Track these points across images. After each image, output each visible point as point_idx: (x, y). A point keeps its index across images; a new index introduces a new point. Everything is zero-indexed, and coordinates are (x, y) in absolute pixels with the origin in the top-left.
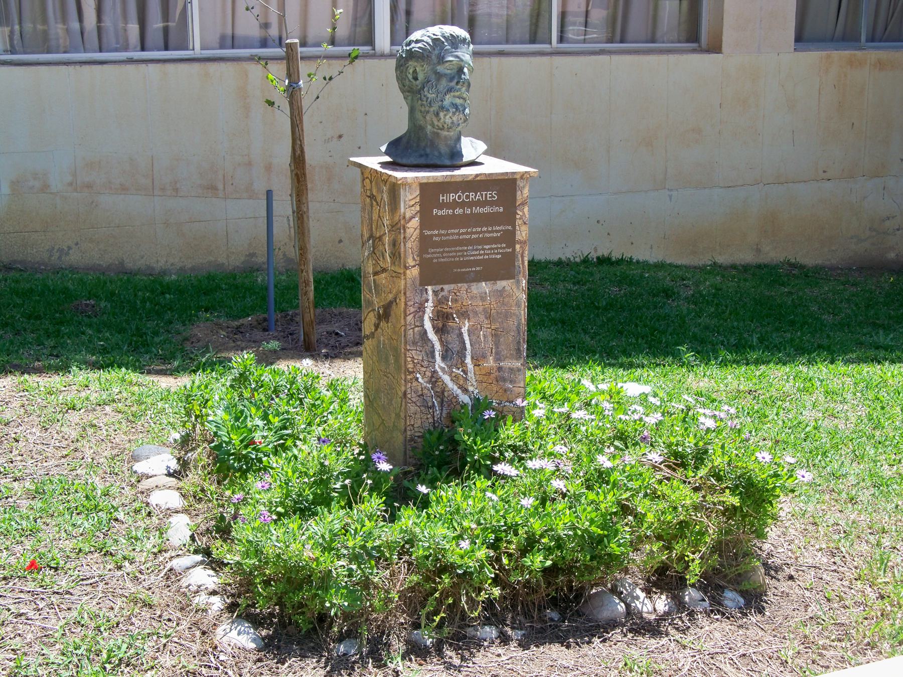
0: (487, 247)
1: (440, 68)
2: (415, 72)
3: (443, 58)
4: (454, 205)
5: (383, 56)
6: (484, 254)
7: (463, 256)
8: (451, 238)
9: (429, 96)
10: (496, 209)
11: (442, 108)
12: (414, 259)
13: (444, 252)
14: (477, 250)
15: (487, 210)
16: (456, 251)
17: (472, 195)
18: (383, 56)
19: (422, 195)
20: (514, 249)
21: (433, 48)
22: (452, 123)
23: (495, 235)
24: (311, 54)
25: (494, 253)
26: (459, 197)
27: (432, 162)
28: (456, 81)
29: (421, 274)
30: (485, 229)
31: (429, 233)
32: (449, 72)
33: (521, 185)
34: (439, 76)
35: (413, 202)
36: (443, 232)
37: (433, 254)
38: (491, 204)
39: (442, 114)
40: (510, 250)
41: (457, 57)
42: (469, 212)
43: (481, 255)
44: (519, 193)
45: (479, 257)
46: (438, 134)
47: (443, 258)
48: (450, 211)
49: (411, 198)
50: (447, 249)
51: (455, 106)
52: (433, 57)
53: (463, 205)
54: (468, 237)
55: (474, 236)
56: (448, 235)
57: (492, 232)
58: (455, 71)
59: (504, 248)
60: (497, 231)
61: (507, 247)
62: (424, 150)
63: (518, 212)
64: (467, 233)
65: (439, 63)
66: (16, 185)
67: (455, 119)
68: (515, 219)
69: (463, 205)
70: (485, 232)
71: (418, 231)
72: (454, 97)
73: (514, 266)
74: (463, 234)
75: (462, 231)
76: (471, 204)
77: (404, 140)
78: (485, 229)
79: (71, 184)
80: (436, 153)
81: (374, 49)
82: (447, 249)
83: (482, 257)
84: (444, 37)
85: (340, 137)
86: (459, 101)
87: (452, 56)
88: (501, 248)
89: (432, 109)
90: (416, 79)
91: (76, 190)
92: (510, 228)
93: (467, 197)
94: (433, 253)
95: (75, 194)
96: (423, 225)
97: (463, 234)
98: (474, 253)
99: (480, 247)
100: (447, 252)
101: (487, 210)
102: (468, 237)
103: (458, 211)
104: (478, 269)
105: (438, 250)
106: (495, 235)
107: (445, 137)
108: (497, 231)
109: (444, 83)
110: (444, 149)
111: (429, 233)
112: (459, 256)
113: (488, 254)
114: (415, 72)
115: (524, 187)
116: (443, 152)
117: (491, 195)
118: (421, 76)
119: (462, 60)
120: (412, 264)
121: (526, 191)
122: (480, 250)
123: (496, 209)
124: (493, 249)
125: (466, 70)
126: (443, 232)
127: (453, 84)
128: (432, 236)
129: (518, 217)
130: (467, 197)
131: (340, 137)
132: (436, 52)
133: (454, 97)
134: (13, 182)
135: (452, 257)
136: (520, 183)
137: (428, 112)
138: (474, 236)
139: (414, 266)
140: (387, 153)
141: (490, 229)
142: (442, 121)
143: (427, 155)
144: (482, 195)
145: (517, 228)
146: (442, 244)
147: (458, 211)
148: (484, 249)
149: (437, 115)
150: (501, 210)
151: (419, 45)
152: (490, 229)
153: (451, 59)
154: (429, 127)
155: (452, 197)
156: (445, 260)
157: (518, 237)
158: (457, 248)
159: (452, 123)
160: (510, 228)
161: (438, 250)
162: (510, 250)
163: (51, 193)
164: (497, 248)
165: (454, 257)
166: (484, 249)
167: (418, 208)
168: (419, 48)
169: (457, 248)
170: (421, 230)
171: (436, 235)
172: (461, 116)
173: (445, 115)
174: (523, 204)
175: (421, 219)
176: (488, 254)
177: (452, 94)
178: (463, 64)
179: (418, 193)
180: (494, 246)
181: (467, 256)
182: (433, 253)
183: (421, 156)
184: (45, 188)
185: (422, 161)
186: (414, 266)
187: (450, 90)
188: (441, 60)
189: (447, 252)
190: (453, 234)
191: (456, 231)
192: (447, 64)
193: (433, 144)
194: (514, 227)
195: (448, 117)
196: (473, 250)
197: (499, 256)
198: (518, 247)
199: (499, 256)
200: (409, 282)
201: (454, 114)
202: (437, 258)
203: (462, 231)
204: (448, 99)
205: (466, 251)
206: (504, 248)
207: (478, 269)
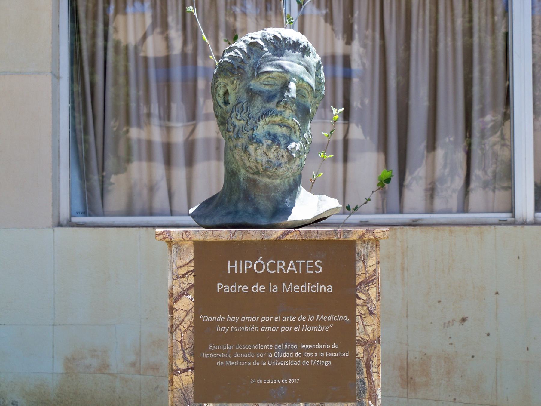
0: (307, 347)
1: (255, 84)
2: (226, 93)
3: (259, 68)
4: (251, 278)
5: (524, 223)
6: (302, 359)
7: (266, 359)
8: (246, 329)
9: (237, 123)
10: (320, 288)
11: (252, 139)
12: (185, 360)
13: (232, 352)
14: (289, 351)
15: (305, 288)
16: (255, 351)
17: (281, 265)
18: (524, 223)
19: (197, 260)
20: (353, 354)
21: (248, 56)
22: (269, 162)
23: (320, 328)
24: (434, 222)
25: (319, 358)
26: (259, 267)
27: (240, 221)
28: (276, 101)
29: (196, 382)
30: (302, 318)
31: (209, 319)
32: (267, 88)
33: (364, 252)
34: (252, 94)
35: (183, 271)
36: (233, 319)
37: (217, 352)
38: (313, 279)
39: (251, 148)
40: (347, 354)
41: (280, 67)
42: (276, 289)
43: (297, 359)
44: (359, 265)
45: (292, 363)
46: (255, 181)
47: (233, 359)
48: (245, 288)
49: (180, 263)
50: (238, 347)
51: (274, 138)
52: (247, 69)
53: (265, 279)
54: (275, 329)
55: (283, 329)
56: (240, 324)
57: (315, 323)
58: (277, 88)
59: (335, 351)
60: (323, 323)
61: (342, 349)
62: (236, 205)
63: (360, 295)
64: (272, 323)
65: (253, 76)
66: (70, 362)
67: (272, 155)
68: (355, 305)
69: (265, 279)
70: (302, 323)
71: (191, 316)
72: (274, 123)
73: (355, 380)
74: (266, 324)
75: (264, 319)
76: (279, 279)
77: (219, 196)
78: (302, 318)
79: (133, 365)
80: (250, 209)
81: (514, 216)
82: (238, 347)
83: (298, 363)
84: (264, 40)
85: (464, 320)
86: (278, 130)
87: (272, 65)
88: (331, 350)
89: (240, 143)
90: (226, 103)
91: (139, 372)
92: (345, 319)
93: (273, 267)
94: (215, 351)
95: (137, 376)
96: (200, 307)
97: (266, 324)
98: (284, 355)
99: (295, 347)
100: (240, 351)
101: (305, 288)
102: (275, 329)
103: (258, 288)
104: (292, 381)
105: (225, 347)
106: (320, 328)
107: (266, 185)
108: (323, 323)
109: (258, 103)
110: (264, 204)
111: (209, 319)
112: (260, 359)
113: (309, 359)
114: (226, 93)
115: (368, 255)
116: (262, 208)
117: (313, 266)
118: (232, 99)
119: (287, 72)
120: (183, 366)
121: (372, 262)
122: (295, 351)
123: (320, 288)
124: (318, 351)
125: (292, 86)
126: (233, 319)
127: (272, 105)
128: (215, 324)
129: (358, 302)
130: (273, 267)
131: (464, 320)
132: (252, 61)
133: (274, 123)
134: (67, 359)
135: (248, 359)
136: (361, 249)
137: (235, 147)
138: (283, 329)
139: (186, 370)
140: (193, 215)
141: (311, 319)
142: (253, 158)
143: (236, 212)
144: (297, 265)
145: (358, 320)
146: (230, 338)
147: (258, 288)
148: (302, 351)
149: (245, 150)
150: (330, 289)
151: (232, 53)
152: (311, 319)
153: (269, 69)
154: (243, 171)
155: (248, 265)
156: (237, 363)
157: (360, 334)
158: (257, 347)
159: (269, 162)
160: (345, 319)
161: (225, 347)
162: (347, 354)
163: (110, 374)
164: (324, 350)
165: (251, 360)
166: (302, 351)
167: (191, 280)
168: (230, 57)
169: (257, 347)
170: (196, 313)
171: (221, 324)
172: (283, 151)
173: (256, 149)
174: (368, 282)
175: (196, 296)
176: (309, 359)
177: (268, 119)
178: (288, 77)
179: (192, 256)
180: (318, 346)
181: (273, 359)
182: (215, 351)
183: (229, 213)
184: (104, 368)
185: (228, 220)
186: (186, 370)
187: (265, 114)
188: (257, 72)
189: (240, 351)
190: (249, 324)
191: (255, 319)
192: (264, 77)
193: (247, 197)
194: (352, 317)
195: (260, 152)
196: (283, 351)
197: (327, 363)
198: (360, 350)
199: (327, 363)
200: (178, 394)
201: (269, 147)
202: (223, 359)
203: (264, 319)
204: (262, 128)
205: (273, 351)
206: (335, 351)
207: (292, 381)
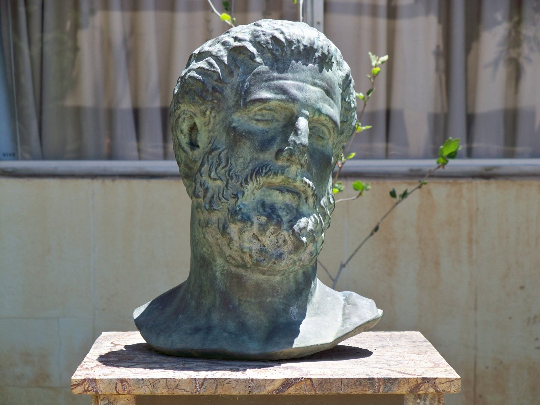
1: (239, 119)
2: (193, 128)
3: (248, 92)
9: (210, 184)
21: (229, 70)
22: (262, 250)
27: (214, 347)
28: (275, 148)
32: (261, 126)
34: (235, 135)
39: (234, 229)
41: (282, 90)
46: (239, 277)
51: (270, 212)
52: (228, 92)
67: (268, 240)
72: (271, 187)
80: (231, 325)
84: (256, 43)
86: (279, 199)
87: (269, 88)
90: (194, 145)
107: (258, 285)
110: (255, 316)
114: (193, 128)
116: (251, 322)
118: (203, 139)
119: (294, 100)
125: (303, 123)
127: (268, 156)
132: (236, 79)
133: (271, 187)
137: (207, 224)
140: (140, 325)
142: (236, 245)
143: (209, 329)
149: (224, 230)
151: (202, 64)
153: (265, 94)
154: (220, 261)
159: (262, 250)
168: (200, 70)
172: (285, 234)
173: (241, 231)
177: (262, 180)
178: (295, 108)
183: (197, 330)
185: (194, 343)
187: (259, 170)
188: (244, 99)
192: (256, 108)
193: (227, 304)
195: (247, 236)
201: (263, 228)
204: (252, 194)
